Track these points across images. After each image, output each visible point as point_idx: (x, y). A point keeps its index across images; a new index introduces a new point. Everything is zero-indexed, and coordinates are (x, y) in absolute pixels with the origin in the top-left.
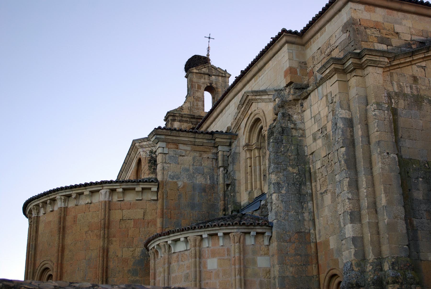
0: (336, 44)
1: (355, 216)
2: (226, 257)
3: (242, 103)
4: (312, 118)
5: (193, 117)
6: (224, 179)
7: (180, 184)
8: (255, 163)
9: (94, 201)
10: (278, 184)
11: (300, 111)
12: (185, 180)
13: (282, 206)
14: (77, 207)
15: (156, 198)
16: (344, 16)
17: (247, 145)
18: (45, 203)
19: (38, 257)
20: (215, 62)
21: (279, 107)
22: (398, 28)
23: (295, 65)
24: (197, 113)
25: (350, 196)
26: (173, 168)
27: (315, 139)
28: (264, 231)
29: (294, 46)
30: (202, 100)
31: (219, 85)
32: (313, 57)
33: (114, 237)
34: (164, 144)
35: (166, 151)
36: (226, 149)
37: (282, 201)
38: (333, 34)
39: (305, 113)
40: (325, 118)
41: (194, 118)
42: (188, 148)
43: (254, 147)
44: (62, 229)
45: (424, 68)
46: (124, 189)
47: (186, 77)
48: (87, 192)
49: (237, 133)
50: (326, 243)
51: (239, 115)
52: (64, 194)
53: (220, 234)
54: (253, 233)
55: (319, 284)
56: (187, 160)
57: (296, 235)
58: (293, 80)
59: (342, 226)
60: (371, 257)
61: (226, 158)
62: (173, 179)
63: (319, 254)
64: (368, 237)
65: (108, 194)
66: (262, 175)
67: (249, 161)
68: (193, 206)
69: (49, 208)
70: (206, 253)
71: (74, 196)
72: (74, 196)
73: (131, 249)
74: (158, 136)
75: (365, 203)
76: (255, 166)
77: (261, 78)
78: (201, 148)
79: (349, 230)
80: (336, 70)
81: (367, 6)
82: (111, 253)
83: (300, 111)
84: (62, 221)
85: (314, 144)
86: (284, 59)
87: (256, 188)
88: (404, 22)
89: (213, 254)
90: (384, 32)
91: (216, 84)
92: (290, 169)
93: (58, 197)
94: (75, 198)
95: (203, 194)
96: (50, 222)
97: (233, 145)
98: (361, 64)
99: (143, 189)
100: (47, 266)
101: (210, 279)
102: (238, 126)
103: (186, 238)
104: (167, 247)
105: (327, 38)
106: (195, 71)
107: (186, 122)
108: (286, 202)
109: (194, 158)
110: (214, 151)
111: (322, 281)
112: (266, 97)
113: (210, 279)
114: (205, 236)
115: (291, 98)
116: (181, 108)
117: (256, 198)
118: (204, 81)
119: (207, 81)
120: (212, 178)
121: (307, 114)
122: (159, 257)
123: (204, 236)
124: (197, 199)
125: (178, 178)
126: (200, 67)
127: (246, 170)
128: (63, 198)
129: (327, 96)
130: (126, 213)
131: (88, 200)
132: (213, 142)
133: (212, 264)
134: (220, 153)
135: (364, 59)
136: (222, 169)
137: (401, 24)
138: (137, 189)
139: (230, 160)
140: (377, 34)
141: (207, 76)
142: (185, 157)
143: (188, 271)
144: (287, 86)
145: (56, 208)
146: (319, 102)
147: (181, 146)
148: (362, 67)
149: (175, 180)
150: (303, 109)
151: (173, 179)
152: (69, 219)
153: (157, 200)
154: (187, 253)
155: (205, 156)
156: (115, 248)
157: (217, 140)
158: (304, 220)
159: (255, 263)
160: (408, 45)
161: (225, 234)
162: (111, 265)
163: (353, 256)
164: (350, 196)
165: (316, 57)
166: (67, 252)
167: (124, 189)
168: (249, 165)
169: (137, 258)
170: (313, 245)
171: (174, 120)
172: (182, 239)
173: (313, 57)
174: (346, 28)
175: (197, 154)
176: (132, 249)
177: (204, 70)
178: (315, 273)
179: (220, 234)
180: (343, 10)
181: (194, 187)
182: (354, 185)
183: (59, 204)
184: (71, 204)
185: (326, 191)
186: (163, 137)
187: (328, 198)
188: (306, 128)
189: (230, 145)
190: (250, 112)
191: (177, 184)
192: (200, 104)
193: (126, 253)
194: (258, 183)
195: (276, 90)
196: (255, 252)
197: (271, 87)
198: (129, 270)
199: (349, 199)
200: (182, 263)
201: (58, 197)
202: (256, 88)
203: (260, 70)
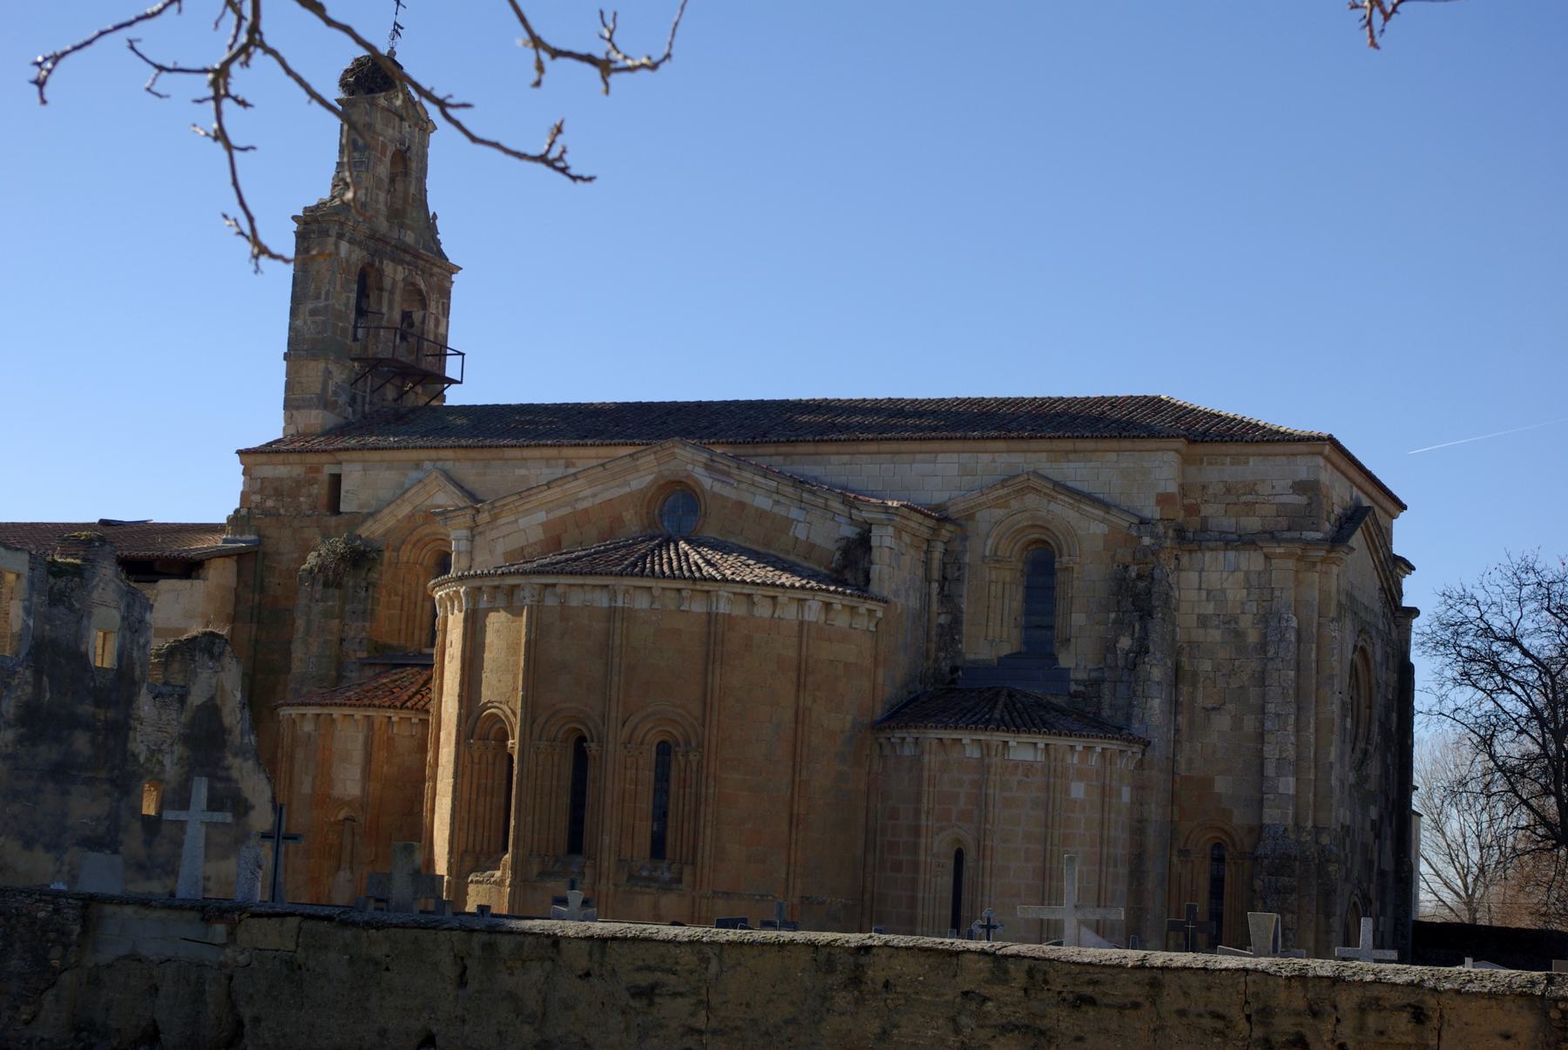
4: (1200, 589)
32: (1204, 487)
60: (1310, 824)
77: (1072, 465)
85: (1201, 631)
107: (360, 244)
118: (388, 133)
119: (397, 135)
129: (1247, 573)
133: (1078, 790)
146: (1225, 575)
165: (1211, 491)
171: (340, 236)
172: (1041, 746)
173: (1204, 487)
174: (1300, 487)
179: (1099, 749)
187: (1222, 722)
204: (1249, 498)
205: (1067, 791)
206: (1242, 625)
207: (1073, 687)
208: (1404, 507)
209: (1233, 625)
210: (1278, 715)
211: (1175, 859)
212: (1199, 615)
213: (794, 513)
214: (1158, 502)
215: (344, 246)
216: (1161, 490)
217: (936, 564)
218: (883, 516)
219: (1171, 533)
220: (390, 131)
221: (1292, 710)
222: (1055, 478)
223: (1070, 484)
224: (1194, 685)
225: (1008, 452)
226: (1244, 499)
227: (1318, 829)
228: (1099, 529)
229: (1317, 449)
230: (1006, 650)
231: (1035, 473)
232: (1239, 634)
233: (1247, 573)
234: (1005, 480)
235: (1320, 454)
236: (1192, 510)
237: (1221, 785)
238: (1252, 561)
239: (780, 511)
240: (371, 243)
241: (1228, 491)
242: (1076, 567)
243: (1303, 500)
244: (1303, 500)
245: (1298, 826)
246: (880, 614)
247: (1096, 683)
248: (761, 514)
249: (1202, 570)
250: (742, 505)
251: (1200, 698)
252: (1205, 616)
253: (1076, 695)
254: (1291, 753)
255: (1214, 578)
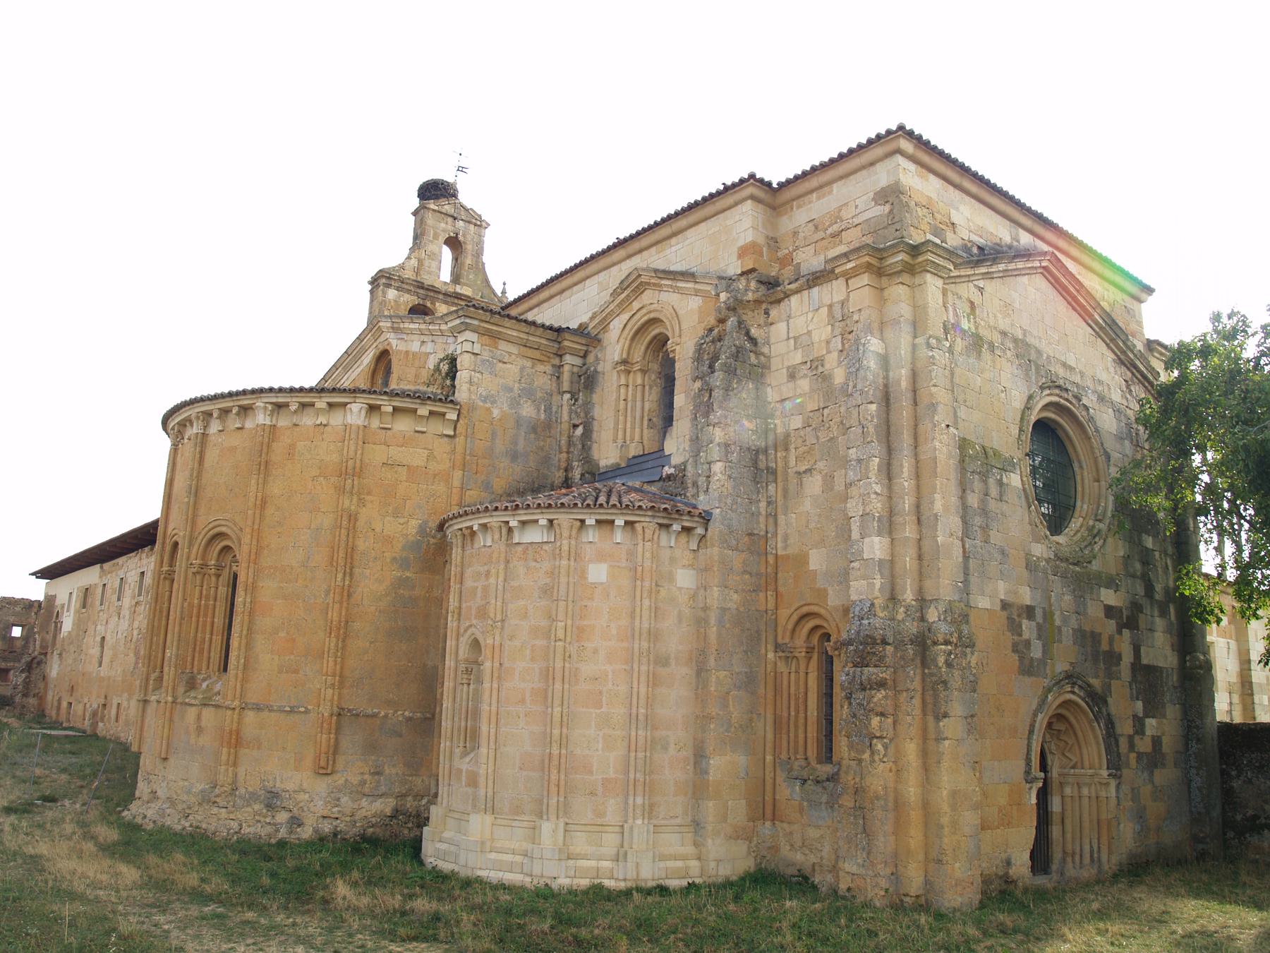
0: (856, 221)
1: (889, 524)
2: (624, 563)
3: (623, 286)
5: (421, 286)
6: (570, 412)
7: (496, 413)
8: (634, 396)
9: (332, 422)
10: (727, 445)
11: (762, 322)
12: (505, 407)
13: (729, 485)
14: (297, 429)
15: (452, 433)
16: (881, 176)
17: (624, 362)
18: (225, 412)
19: (202, 511)
20: (466, 197)
21: (728, 309)
22: (956, 218)
23: (761, 240)
24: (427, 280)
25: (878, 488)
26: (488, 384)
27: (792, 376)
28: (694, 525)
29: (760, 206)
30: (437, 258)
31: (469, 238)
32: (795, 233)
33: (369, 493)
34: (472, 336)
35: (477, 348)
36: (578, 361)
37: (730, 477)
38: (856, 199)
39: (773, 328)
40: (824, 345)
41: (423, 288)
42: (514, 349)
43: (637, 367)
44: (264, 466)
45: (981, 289)
46: (395, 409)
47: (415, 213)
48: (321, 403)
49: (600, 336)
50: (802, 560)
51: (612, 306)
52: (274, 400)
53: (619, 522)
54: (676, 527)
55: (776, 626)
56: (513, 369)
57: (746, 539)
58: (757, 266)
59: (855, 535)
60: (909, 596)
61: (576, 378)
62: (485, 401)
63: (779, 575)
64: (908, 560)
65: (363, 412)
66: (646, 418)
67: (623, 390)
68: (514, 456)
69: (233, 422)
70: (588, 551)
71: (293, 407)
72: (293, 407)
73: (402, 521)
74: (468, 321)
75: (907, 503)
76: (634, 401)
77: (673, 249)
78: (537, 354)
79: (876, 547)
80: (869, 267)
81: (919, 169)
82: (361, 523)
83: (762, 322)
84: (265, 450)
85: (791, 385)
86: (744, 223)
87: (632, 440)
88: (962, 208)
89: (601, 557)
90: (938, 216)
91: (464, 236)
92: (746, 423)
93: (259, 404)
94: (295, 411)
95: (533, 436)
96: (233, 449)
97: (591, 358)
98: (913, 266)
99: (431, 413)
100: (223, 529)
101: (592, 599)
102: (604, 325)
103: (551, 521)
104: (504, 531)
105: (835, 205)
106: (432, 206)
107: (409, 291)
108: (735, 479)
109: (522, 369)
110: (556, 361)
111: (782, 621)
112: (690, 285)
113: (592, 599)
114: (590, 521)
115: (750, 296)
116: (402, 267)
117: (634, 457)
119: (450, 227)
120: (548, 409)
121: (780, 329)
122: (476, 546)
123: (588, 522)
124: (521, 445)
125: (494, 402)
126: (443, 201)
127: (617, 404)
128: (270, 407)
129: (830, 306)
130: (395, 453)
131: (322, 419)
132: (556, 346)
133: (598, 573)
134: (566, 368)
135: (920, 259)
136: (568, 396)
137: (957, 209)
138: (419, 412)
139: (587, 381)
140: (929, 219)
141: (450, 220)
142: (508, 366)
143: (548, 580)
144: (743, 274)
145: (249, 424)
146: (810, 315)
147: (503, 345)
148: (910, 269)
149: (488, 405)
150: (770, 320)
151: (485, 401)
152: (279, 448)
153: (454, 437)
154: (546, 547)
155: (541, 368)
156: (370, 513)
157: (566, 343)
158: (760, 513)
159: (671, 578)
160: (966, 248)
161: (626, 523)
162: (361, 545)
163: (877, 593)
164: (878, 488)
165: (802, 235)
166: (270, 511)
167: (395, 409)
168: (622, 397)
169: (411, 538)
170: (771, 559)
171: (389, 286)
172: (543, 522)
173: (795, 233)
175: (529, 364)
176: (402, 521)
177: (448, 208)
178: (771, 605)
179: (619, 522)
180: (878, 166)
181: (518, 422)
182: (888, 471)
183: (262, 418)
184: (283, 421)
185: (808, 471)
186: (476, 322)
187: (814, 484)
188: (773, 354)
189: (584, 357)
190: (636, 305)
191: (491, 413)
192: (434, 264)
193: (391, 526)
194: (637, 430)
195: (721, 278)
196: (672, 560)
197: (713, 268)
198: (394, 559)
199: (876, 493)
200: (534, 564)
201: (259, 404)
202: (661, 265)
203: (674, 234)
204: (835, 228)
205: (583, 575)
206: (827, 366)
207: (668, 470)
208: (1149, 290)
209: (820, 369)
210: (859, 461)
211: (771, 655)
212: (788, 368)
213: (429, 348)
214: (740, 256)
215: (392, 294)
216: (741, 243)
217: (566, 376)
218: (458, 321)
219: (753, 284)
220: (443, 225)
221: (877, 448)
222: (662, 267)
223: (672, 269)
224: (787, 449)
225: (629, 256)
226: (830, 231)
227: (923, 602)
228: (695, 303)
229: (891, 146)
230: (634, 450)
231: (647, 269)
232: (826, 378)
233: (830, 306)
234: (622, 282)
235: (899, 151)
236: (786, 261)
237: (816, 561)
238: (834, 292)
239: (424, 349)
240: (421, 291)
241: (816, 227)
242: (678, 348)
243: (887, 208)
244: (887, 208)
245: (893, 598)
246: (452, 416)
247: (685, 464)
248: (414, 354)
249: (789, 317)
250: (407, 352)
251: (792, 462)
252: (794, 367)
253: (669, 477)
254: (877, 506)
255: (799, 325)
